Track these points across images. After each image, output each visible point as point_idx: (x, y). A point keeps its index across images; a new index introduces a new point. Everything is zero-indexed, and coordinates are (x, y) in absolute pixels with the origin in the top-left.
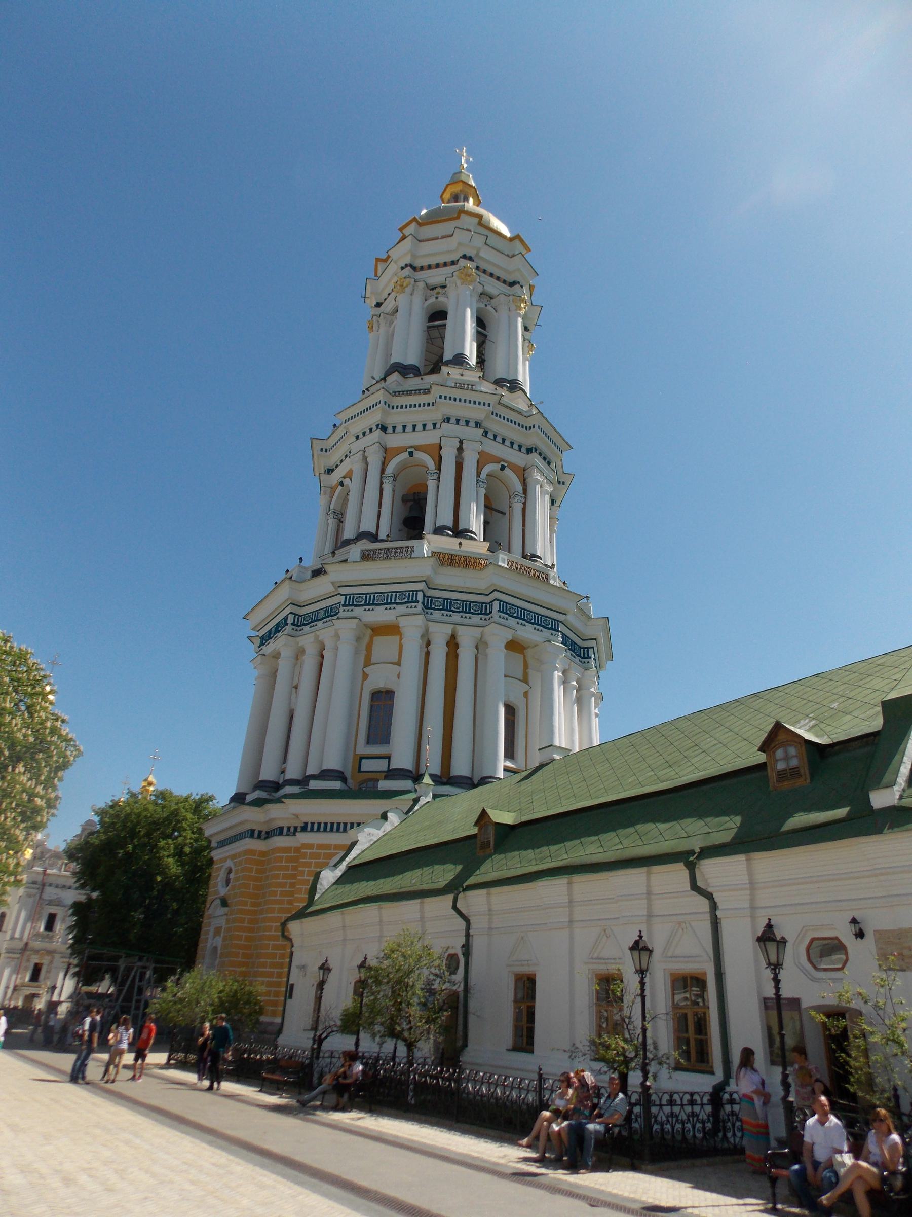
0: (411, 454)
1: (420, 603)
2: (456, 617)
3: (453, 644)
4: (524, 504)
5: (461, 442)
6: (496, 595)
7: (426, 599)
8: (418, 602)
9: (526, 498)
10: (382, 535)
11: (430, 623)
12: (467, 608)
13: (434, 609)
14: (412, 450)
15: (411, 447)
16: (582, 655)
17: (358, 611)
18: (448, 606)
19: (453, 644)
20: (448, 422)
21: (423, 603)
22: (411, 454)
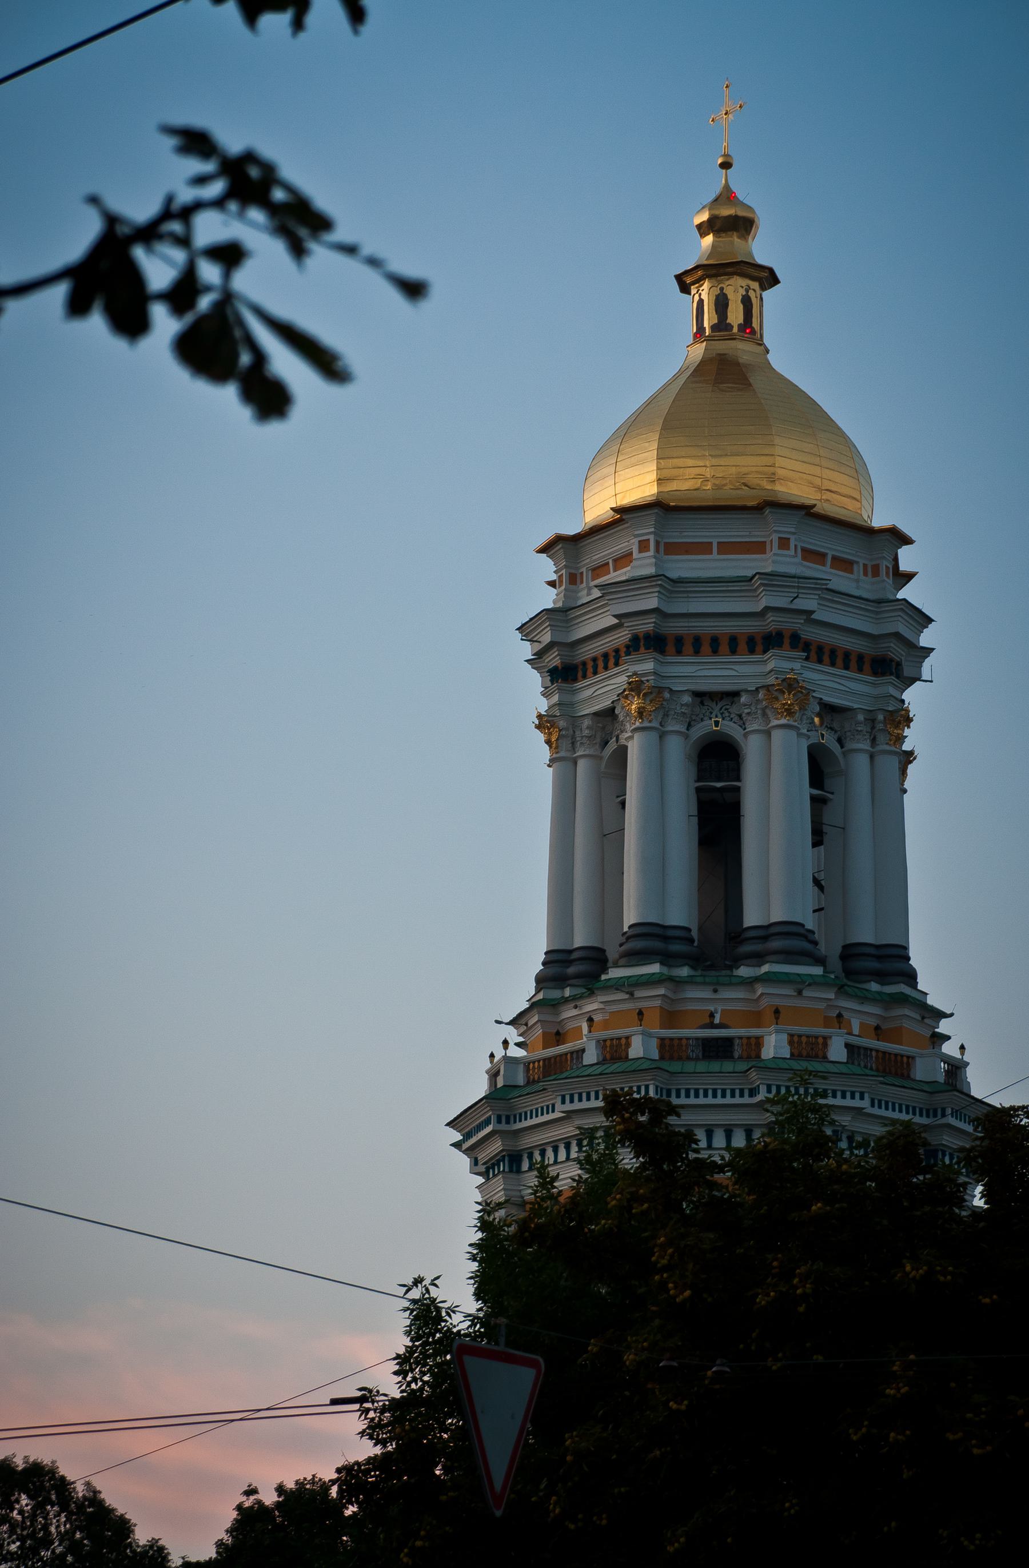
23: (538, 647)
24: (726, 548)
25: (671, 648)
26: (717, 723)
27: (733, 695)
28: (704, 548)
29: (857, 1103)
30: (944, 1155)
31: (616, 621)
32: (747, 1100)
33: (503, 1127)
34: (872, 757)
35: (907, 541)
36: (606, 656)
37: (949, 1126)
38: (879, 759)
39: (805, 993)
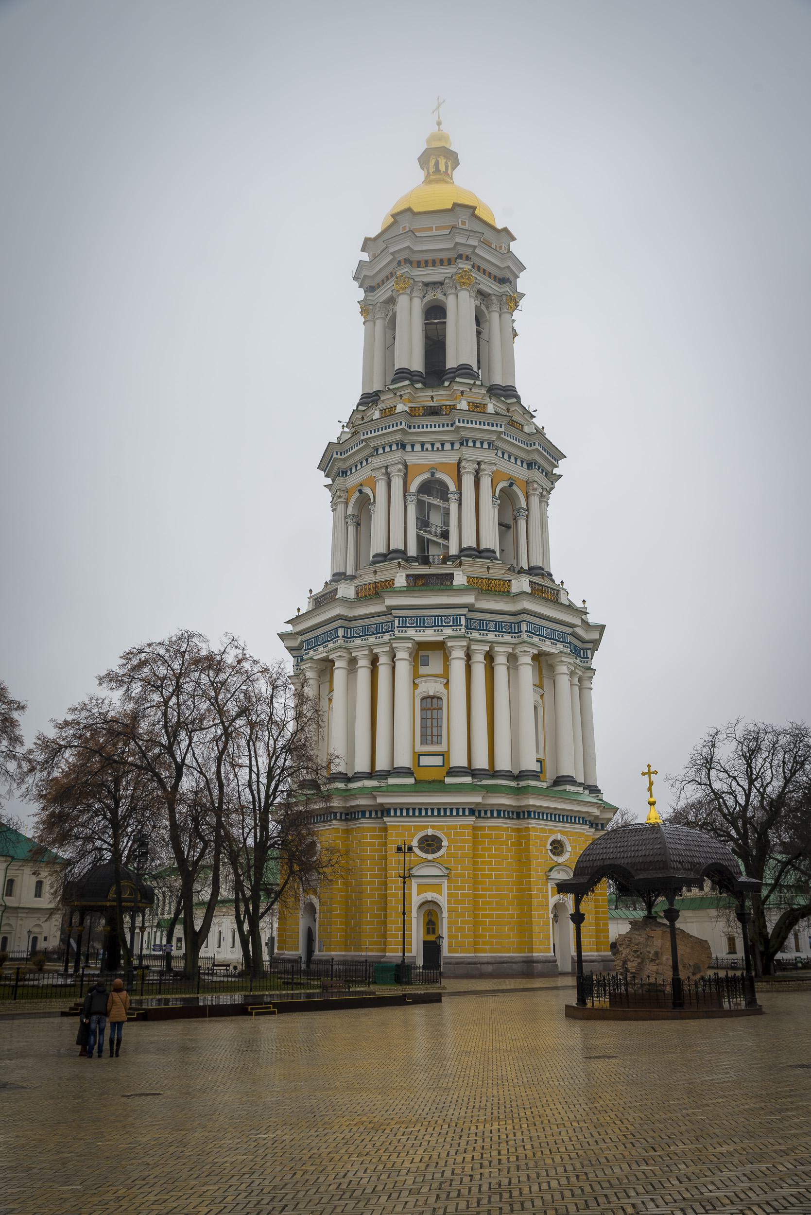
0: (360, 491)
1: (341, 637)
2: (372, 640)
3: (374, 661)
4: (460, 500)
5: (387, 468)
6: (395, 613)
7: (349, 630)
8: (339, 637)
9: (461, 494)
10: (350, 572)
11: (351, 651)
12: (379, 631)
13: (356, 637)
14: (359, 488)
15: (361, 485)
16: (516, 631)
17: (312, 653)
18: (365, 632)
19: (374, 661)
20: (377, 454)
21: (343, 637)
22: (360, 491)
23: (360, 281)
24: (438, 228)
25: (415, 265)
26: (435, 295)
27: (441, 283)
28: (431, 229)
29: (499, 429)
30: (535, 466)
31: (391, 257)
32: (450, 428)
33: (339, 456)
34: (500, 316)
35: (514, 239)
36: (387, 277)
37: (537, 450)
38: (503, 316)
39: (473, 390)
